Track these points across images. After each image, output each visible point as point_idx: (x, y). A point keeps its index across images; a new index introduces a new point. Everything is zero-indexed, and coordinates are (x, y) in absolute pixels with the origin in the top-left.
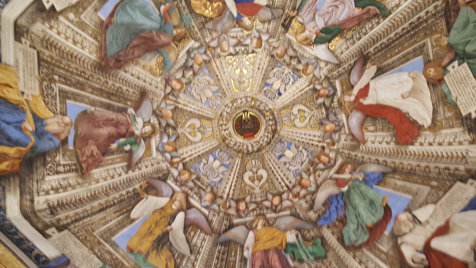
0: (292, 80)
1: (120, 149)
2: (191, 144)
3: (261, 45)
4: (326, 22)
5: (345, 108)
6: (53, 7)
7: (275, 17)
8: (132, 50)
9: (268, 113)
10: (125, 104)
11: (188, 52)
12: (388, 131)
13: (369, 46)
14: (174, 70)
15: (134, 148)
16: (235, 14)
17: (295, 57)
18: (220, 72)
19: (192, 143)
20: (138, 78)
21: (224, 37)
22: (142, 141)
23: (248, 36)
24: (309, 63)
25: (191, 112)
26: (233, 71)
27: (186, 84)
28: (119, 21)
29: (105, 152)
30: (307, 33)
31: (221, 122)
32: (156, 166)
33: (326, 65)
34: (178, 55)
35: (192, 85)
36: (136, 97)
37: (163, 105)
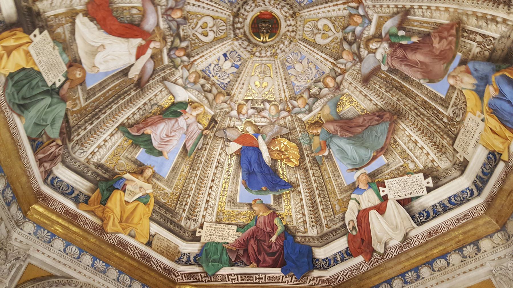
0: (211, 68)
1: (410, 34)
2: (331, 18)
3: (238, 106)
4: (177, 123)
5: (160, 34)
6: (426, 177)
7: (223, 130)
8: (363, 124)
9: (240, 36)
10: (388, 76)
11: (310, 111)
12: (117, 8)
13: (135, 96)
14: (328, 97)
15: (394, 30)
16: (260, 137)
17: (206, 91)
18: (283, 86)
19: (330, 19)
20: (366, 96)
21: (273, 119)
22: (383, 35)
23: (251, 117)
24: (193, 84)
25: (322, 52)
26: (270, 86)
27: (319, 81)
28: (370, 151)
29: (426, 37)
30: (195, 113)
31: (293, 34)
32: (378, 4)
33: (176, 80)
34: (321, 110)
35: (314, 79)
36: (374, 79)
37: (349, 65)
